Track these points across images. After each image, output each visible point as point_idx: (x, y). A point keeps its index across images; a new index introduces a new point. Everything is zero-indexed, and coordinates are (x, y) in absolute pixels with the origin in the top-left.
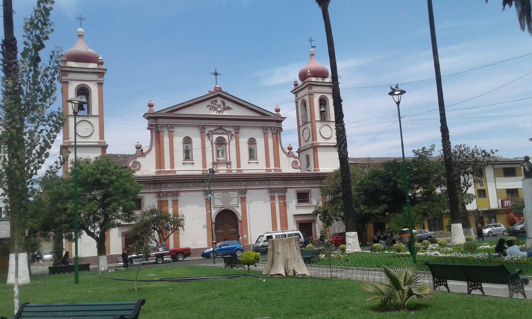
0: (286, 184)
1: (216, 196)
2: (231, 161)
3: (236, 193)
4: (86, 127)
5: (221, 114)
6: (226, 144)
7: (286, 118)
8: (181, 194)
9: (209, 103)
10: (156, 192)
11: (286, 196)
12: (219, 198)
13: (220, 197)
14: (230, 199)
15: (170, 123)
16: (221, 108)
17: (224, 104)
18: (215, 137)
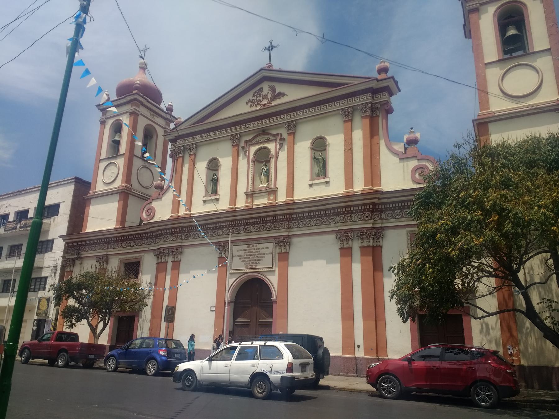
0: (381, 219)
1: (236, 253)
2: (277, 187)
3: (270, 245)
4: (112, 171)
5: (267, 106)
6: (271, 158)
7: (392, 78)
8: (187, 251)
9: (249, 96)
10: (154, 250)
11: (381, 247)
12: (241, 256)
13: (242, 253)
14: (259, 256)
15: (192, 142)
16: (268, 99)
17: (273, 89)
18: (253, 149)
